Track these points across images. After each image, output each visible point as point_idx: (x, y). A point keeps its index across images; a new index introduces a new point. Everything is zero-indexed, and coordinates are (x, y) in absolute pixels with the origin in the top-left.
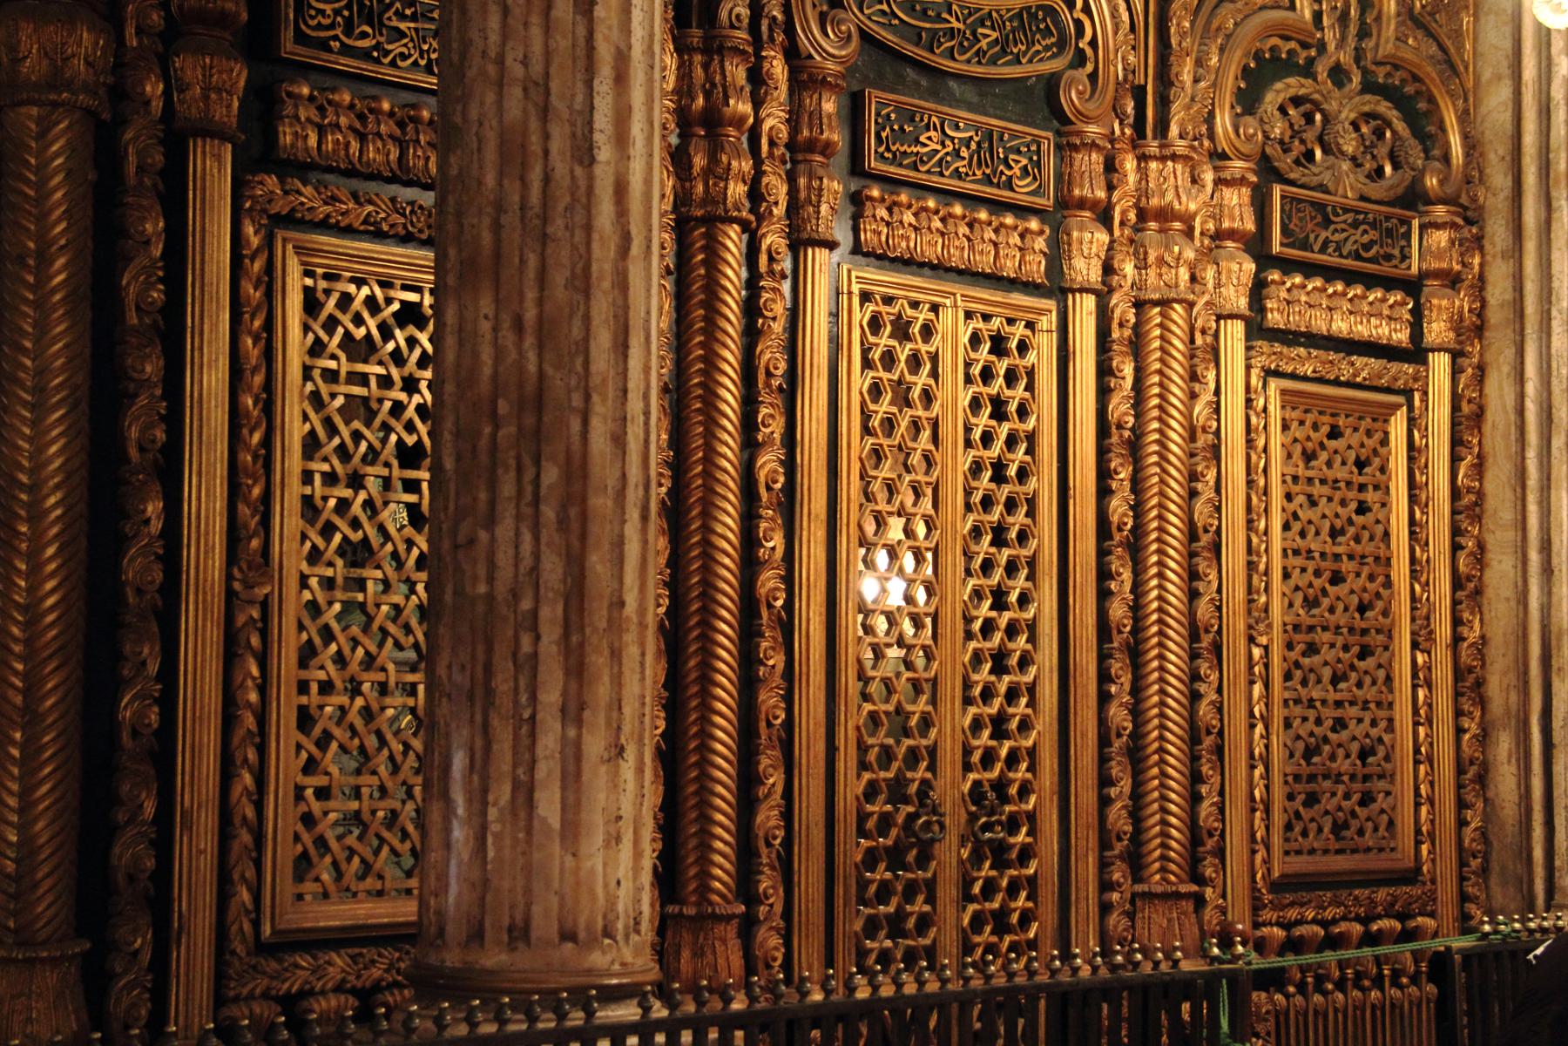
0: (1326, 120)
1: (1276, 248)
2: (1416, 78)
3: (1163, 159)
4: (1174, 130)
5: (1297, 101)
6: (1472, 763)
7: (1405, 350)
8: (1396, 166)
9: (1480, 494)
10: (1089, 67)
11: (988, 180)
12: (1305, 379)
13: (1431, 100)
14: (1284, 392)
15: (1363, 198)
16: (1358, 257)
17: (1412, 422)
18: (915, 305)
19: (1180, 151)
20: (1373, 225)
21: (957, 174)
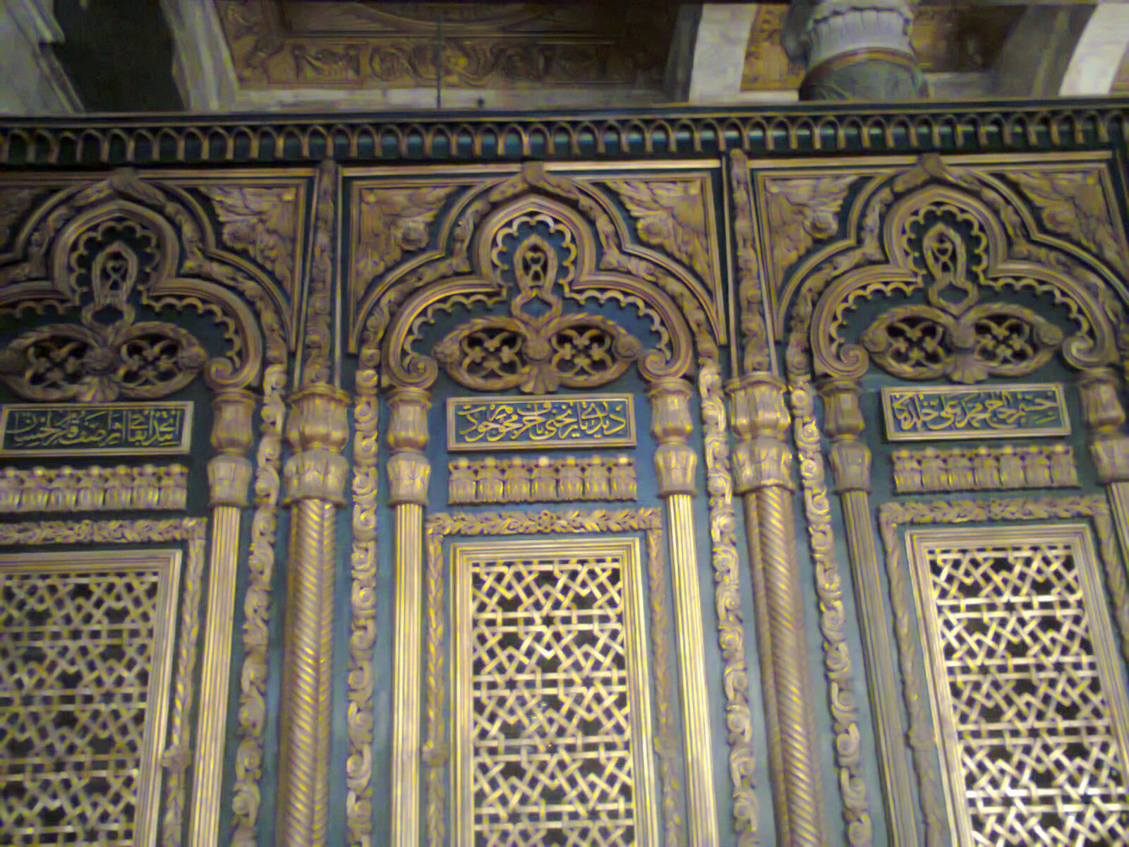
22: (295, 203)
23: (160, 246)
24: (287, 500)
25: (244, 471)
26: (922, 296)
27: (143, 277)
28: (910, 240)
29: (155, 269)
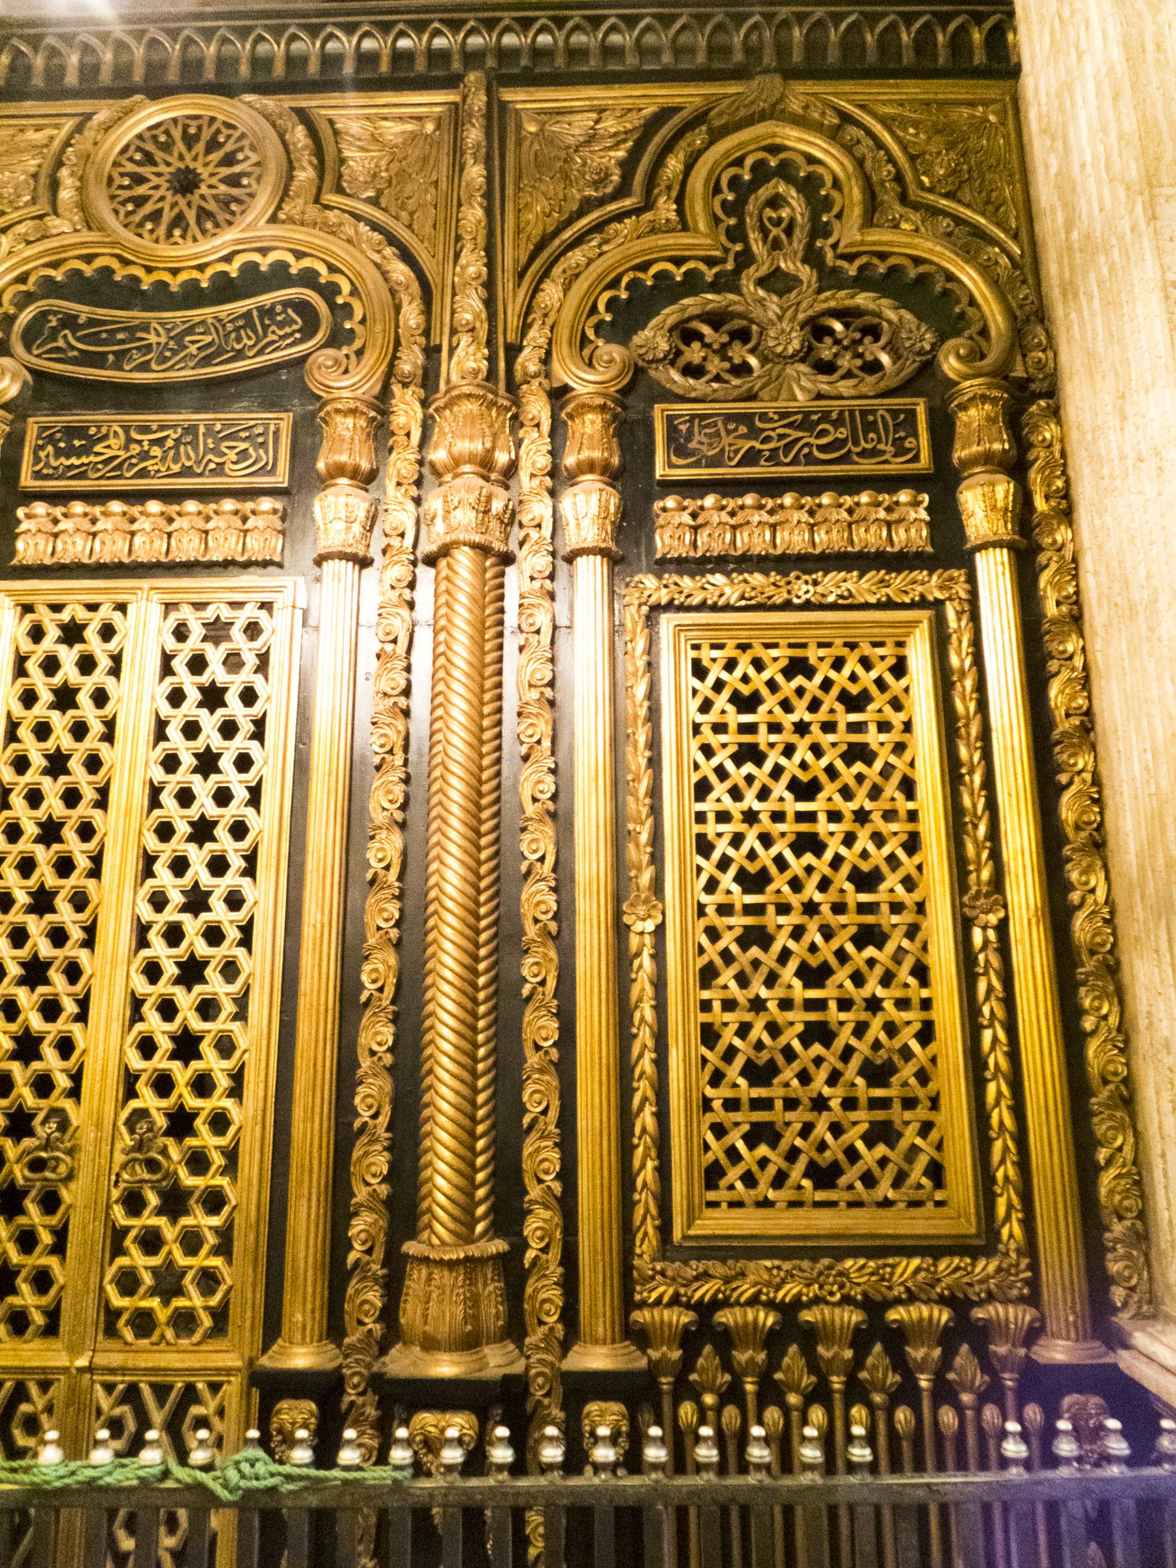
2: (917, 261)
4: (454, 378)
5: (716, 319)
6: (1105, 1082)
8: (896, 356)
9: (1089, 713)
10: (358, 344)
11: (187, 472)
12: (728, 608)
13: (950, 277)
14: (680, 628)
16: (810, 460)
17: (940, 642)
19: (466, 390)
20: (838, 423)
28: (724, 203)
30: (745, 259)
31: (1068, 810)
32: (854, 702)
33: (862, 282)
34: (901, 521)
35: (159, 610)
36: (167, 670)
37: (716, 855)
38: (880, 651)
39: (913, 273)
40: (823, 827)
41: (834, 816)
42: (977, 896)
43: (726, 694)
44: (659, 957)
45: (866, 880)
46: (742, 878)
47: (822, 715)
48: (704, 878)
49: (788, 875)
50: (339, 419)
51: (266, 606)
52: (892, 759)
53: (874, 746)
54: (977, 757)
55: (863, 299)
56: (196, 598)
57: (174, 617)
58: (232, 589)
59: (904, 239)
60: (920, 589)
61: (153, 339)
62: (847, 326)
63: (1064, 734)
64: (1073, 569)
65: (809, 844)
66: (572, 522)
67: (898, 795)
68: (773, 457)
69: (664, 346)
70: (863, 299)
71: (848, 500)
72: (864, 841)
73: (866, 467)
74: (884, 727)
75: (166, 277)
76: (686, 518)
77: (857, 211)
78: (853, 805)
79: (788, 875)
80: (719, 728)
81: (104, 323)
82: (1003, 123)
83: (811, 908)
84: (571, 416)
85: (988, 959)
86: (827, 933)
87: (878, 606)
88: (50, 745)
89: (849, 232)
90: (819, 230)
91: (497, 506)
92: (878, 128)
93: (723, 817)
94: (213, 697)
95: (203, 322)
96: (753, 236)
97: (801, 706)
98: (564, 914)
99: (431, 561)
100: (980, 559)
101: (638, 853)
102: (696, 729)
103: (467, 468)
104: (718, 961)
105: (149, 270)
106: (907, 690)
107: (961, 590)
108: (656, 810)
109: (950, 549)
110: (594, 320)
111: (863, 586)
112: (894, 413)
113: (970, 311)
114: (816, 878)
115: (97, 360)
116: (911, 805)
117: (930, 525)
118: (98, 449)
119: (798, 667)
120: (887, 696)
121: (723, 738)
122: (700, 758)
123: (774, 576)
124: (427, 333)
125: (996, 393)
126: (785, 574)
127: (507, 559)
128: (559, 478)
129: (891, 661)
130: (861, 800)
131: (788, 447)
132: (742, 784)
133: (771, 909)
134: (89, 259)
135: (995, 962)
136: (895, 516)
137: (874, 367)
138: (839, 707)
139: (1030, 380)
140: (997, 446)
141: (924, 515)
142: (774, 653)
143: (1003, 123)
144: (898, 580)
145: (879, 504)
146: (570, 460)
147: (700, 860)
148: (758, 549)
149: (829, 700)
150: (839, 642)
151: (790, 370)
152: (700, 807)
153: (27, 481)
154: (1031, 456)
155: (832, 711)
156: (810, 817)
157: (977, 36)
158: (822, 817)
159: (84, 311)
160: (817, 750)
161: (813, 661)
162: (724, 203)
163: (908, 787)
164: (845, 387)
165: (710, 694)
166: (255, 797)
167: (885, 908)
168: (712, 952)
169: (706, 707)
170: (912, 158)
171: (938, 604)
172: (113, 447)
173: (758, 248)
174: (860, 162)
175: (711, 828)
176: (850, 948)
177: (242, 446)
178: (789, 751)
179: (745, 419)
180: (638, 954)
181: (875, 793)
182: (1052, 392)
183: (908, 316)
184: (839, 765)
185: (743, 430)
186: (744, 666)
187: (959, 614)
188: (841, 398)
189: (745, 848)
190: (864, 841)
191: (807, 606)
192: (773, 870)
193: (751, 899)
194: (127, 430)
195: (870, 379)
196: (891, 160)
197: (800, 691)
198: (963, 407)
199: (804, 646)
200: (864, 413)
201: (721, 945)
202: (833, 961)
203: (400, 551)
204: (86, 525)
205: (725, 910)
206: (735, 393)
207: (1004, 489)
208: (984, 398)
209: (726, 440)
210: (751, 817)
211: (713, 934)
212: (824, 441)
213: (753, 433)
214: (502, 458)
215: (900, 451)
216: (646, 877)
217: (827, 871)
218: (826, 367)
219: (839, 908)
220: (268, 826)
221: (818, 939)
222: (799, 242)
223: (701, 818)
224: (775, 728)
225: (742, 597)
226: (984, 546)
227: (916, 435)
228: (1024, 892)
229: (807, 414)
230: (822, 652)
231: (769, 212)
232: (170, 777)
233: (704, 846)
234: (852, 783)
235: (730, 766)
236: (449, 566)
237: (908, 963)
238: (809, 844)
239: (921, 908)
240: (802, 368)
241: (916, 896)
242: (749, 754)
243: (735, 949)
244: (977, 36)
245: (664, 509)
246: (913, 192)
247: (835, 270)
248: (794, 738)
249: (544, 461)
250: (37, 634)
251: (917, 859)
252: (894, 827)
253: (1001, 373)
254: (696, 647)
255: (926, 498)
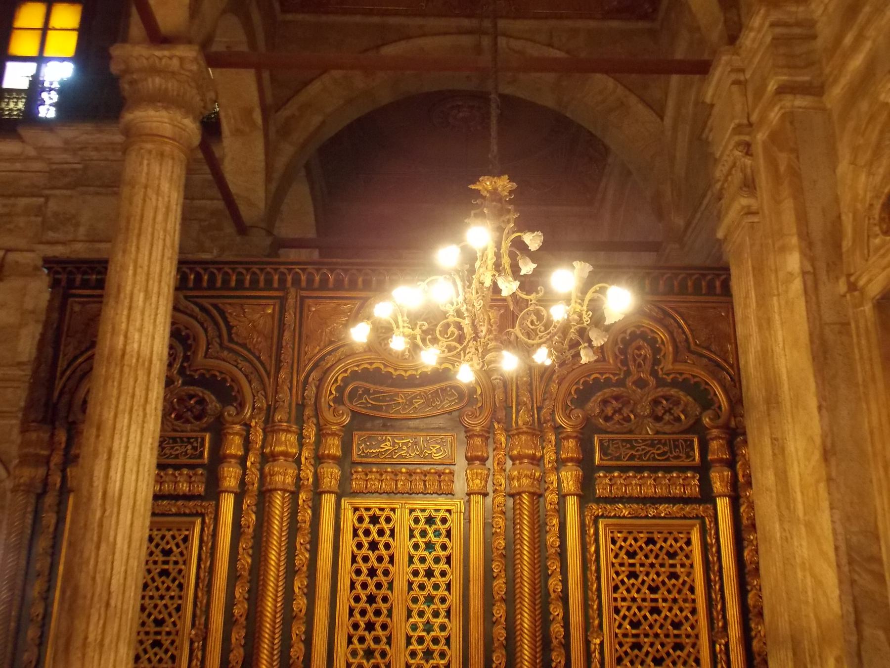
0: (635, 404)
1: (597, 461)
2: (694, 376)
3: (518, 434)
5: (617, 398)
7: (696, 498)
12: (624, 517)
13: (707, 383)
14: (606, 525)
15: (657, 433)
16: (655, 459)
18: (382, 509)
20: (665, 445)
21: (401, 456)
22: (272, 315)
23: (195, 339)
24: (264, 489)
25: (239, 471)
26: (621, 383)
27: (186, 358)
29: (194, 352)
30: (628, 373)
31: (751, 599)
32: (672, 555)
33: (674, 384)
34: (688, 485)
35: (407, 511)
36: (412, 536)
37: (622, 614)
38: (681, 536)
39: (692, 382)
40: (661, 604)
41: (665, 600)
42: (718, 632)
43: (624, 551)
44: (602, 653)
45: (677, 625)
46: (631, 623)
47: (660, 560)
48: (617, 623)
49: (648, 622)
50: (476, 439)
51: (449, 511)
52: (686, 578)
53: (679, 573)
54: (717, 578)
55: (673, 392)
56: (422, 507)
57: (414, 514)
58: (435, 504)
59: (688, 368)
60: (695, 511)
61: (401, 401)
62: (667, 400)
63: (749, 571)
64: (751, 506)
65: (655, 610)
66: (565, 482)
67: (688, 593)
68: (640, 458)
69: (598, 410)
70: (673, 392)
71: (668, 476)
72: (676, 610)
73: (675, 463)
74: (683, 565)
75: (403, 373)
76: (607, 481)
77: (671, 357)
78: (671, 596)
79: (648, 622)
80: (622, 565)
81: (382, 392)
82: (727, 316)
83: (657, 635)
84: (564, 439)
85: (721, 656)
86: (663, 645)
87: (681, 518)
88: (369, 564)
89: (668, 364)
90: (656, 362)
91: (537, 474)
92: (679, 319)
93: (624, 599)
94: (430, 546)
95: (420, 394)
96: (631, 363)
97: (652, 556)
98: (567, 635)
99: (512, 495)
100: (718, 500)
101: (593, 613)
102: (613, 564)
103: (526, 461)
104: (623, 655)
105: (396, 370)
106: (691, 551)
107: (711, 512)
108: (599, 597)
109: (707, 497)
110: (570, 398)
111: (675, 509)
112: (685, 441)
113: (715, 398)
114: (658, 624)
115: (379, 408)
116: (693, 597)
117: (699, 487)
118: (382, 446)
119: (651, 541)
120: (684, 553)
121: (623, 569)
122: (615, 576)
123: (641, 506)
124: (506, 401)
125: (723, 436)
126: (644, 504)
127: (540, 496)
128: (560, 463)
129: (685, 540)
130: (675, 594)
131: (645, 454)
132: (630, 587)
133: (642, 636)
134: (371, 364)
135: (724, 658)
136: (686, 482)
137: (678, 419)
138: (666, 557)
139: (737, 428)
140: (724, 457)
141: (697, 482)
142: (642, 535)
143: (727, 316)
144: (688, 508)
145: (679, 477)
146: (564, 456)
147: (615, 616)
148: (635, 494)
149: (662, 555)
150: (666, 531)
151: (646, 421)
152: (615, 595)
153: (355, 458)
154: (738, 458)
155: (663, 559)
156: (656, 600)
157: (718, 283)
158: (660, 600)
159: (372, 388)
160: (658, 574)
161: (656, 539)
162: (619, 348)
163: (692, 590)
164: (667, 428)
165: (618, 551)
166: (448, 587)
167: (684, 636)
168: (621, 652)
169: (616, 556)
170: (691, 330)
171: (703, 518)
172: (387, 446)
173: (633, 368)
174: (671, 333)
175: (620, 604)
176: (671, 651)
177: (438, 446)
178: (647, 574)
179: (629, 441)
180: (594, 651)
181: (679, 592)
182: (744, 434)
183: (691, 399)
184: (666, 580)
185: (628, 445)
186: (630, 541)
187: (710, 522)
188: (665, 433)
189: (632, 612)
190: (676, 610)
191: (654, 517)
192: (643, 620)
193: (634, 632)
194: (393, 438)
195: (677, 424)
196: (684, 332)
197: (651, 551)
198: (713, 439)
199: (652, 533)
200: (674, 441)
201: (624, 649)
202: (665, 656)
203: (501, 491)
204: (378, 476)
205: (625, 635)
206: (625, 430)
207: (727, 473)
208: (720, 438)
209: (622, 450)
210: (634, 600)
211: (621, 645)
212: (659, 452)
213: (632, 447)
214: (538, 454)
215: (688, 456)
216: (596, 622)
217: (662, 621)
218: (658, 419)
219: (667, 636)
220: (454, 599)
221: (659, 647)
222: (649, 363)
223: (615, 599)
224: (642, 565)
225: (629, 513)
226: (720, 496)
227: (693, 450)
228: (734, 631)
229: (653, 440)
230: (659, 536)
231: (636, 351)
232: (416, 579)
233: (617, 611)
234: (671, 587)
235: (626, 580)
236: (520, 499)
237: (692, 657)
238: (655, 610)
239: (697, 636)
240: (650, 420)
241: (695, 631)
242: (633, 575)
243: (629, 650)
244: (718, 283)
245: (600, 477)
246: (693, 347)
247: (663, 378)
248: (650, 569)
249: (553, 457)
250: (361, 520)
251: (695, 617)
252: (687, 605)
253: (726, 427)
254: (612, 532)
255: (698, 476)
